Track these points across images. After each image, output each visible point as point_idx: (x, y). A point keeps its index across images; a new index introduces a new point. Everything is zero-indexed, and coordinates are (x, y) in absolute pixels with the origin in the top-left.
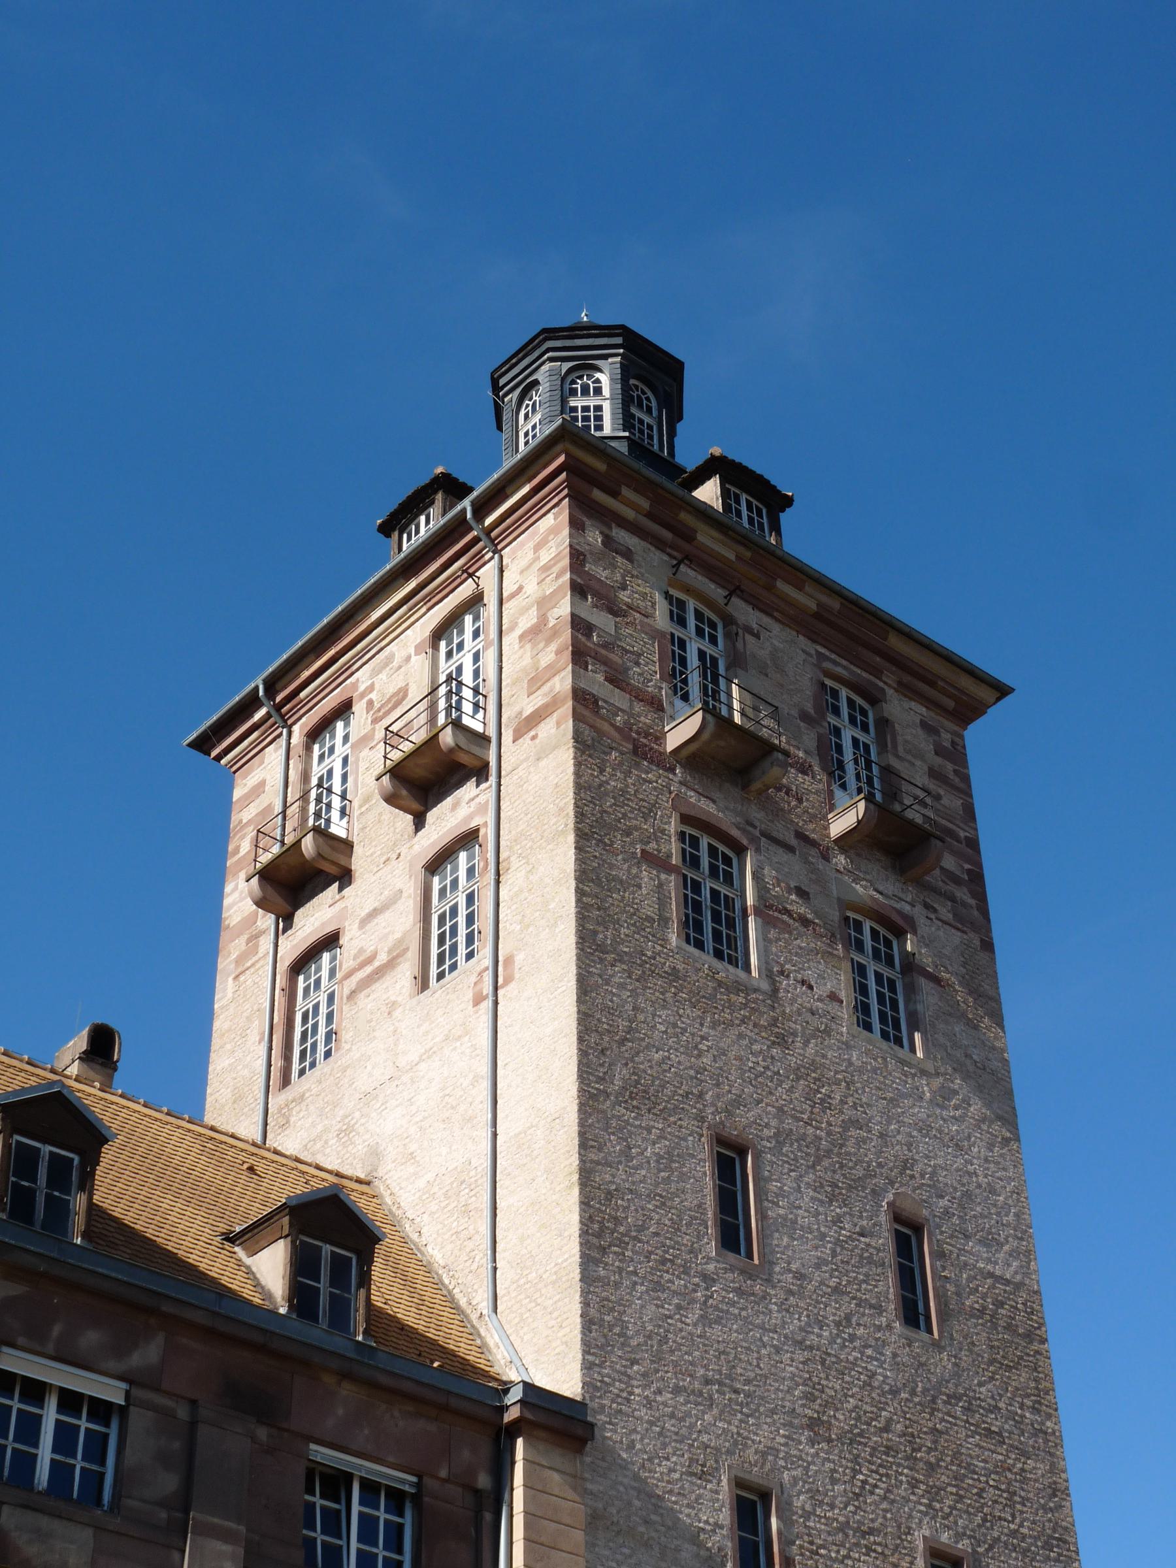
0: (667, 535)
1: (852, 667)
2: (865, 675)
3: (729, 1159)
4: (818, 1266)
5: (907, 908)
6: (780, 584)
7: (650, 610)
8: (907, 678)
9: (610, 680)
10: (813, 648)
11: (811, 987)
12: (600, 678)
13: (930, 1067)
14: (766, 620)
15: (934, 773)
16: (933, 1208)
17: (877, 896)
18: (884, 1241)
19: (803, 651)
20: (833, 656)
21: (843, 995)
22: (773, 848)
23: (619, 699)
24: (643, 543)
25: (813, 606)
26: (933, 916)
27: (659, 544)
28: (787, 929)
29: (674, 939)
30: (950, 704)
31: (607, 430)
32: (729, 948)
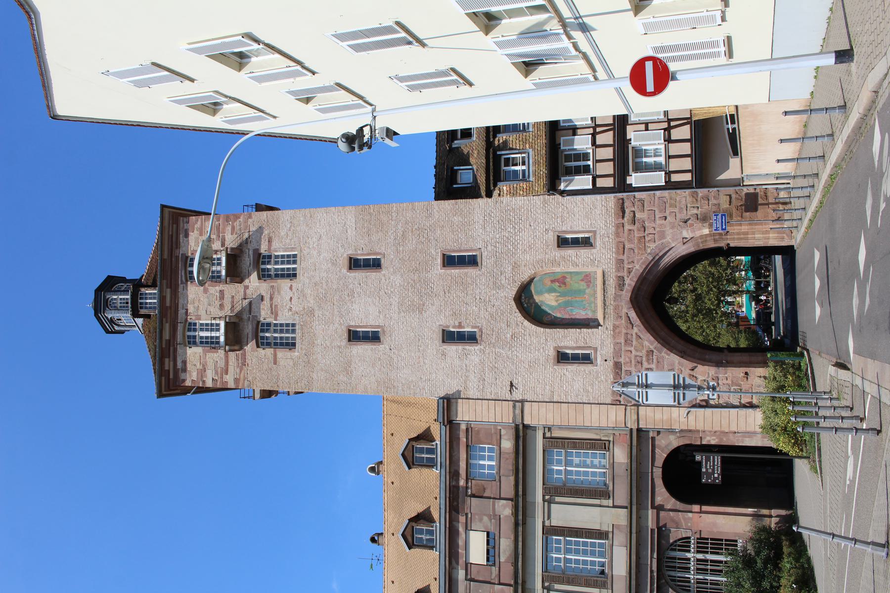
0: (172, 348)
3: (354, 336)
5: (251, 253)
6: (168, 304)
8: (174, 246)
9: (227, 374)
10: (181, 286)
13: (299, 248)
14: (180, 306)
16: (344, 254)
18: (359, 275)
25: (169, 290)
27: (175, 350)
28: (276, 306)
29: (296, 354)
30: (175, 226)
31: (129, 297)
32: (291, 327)
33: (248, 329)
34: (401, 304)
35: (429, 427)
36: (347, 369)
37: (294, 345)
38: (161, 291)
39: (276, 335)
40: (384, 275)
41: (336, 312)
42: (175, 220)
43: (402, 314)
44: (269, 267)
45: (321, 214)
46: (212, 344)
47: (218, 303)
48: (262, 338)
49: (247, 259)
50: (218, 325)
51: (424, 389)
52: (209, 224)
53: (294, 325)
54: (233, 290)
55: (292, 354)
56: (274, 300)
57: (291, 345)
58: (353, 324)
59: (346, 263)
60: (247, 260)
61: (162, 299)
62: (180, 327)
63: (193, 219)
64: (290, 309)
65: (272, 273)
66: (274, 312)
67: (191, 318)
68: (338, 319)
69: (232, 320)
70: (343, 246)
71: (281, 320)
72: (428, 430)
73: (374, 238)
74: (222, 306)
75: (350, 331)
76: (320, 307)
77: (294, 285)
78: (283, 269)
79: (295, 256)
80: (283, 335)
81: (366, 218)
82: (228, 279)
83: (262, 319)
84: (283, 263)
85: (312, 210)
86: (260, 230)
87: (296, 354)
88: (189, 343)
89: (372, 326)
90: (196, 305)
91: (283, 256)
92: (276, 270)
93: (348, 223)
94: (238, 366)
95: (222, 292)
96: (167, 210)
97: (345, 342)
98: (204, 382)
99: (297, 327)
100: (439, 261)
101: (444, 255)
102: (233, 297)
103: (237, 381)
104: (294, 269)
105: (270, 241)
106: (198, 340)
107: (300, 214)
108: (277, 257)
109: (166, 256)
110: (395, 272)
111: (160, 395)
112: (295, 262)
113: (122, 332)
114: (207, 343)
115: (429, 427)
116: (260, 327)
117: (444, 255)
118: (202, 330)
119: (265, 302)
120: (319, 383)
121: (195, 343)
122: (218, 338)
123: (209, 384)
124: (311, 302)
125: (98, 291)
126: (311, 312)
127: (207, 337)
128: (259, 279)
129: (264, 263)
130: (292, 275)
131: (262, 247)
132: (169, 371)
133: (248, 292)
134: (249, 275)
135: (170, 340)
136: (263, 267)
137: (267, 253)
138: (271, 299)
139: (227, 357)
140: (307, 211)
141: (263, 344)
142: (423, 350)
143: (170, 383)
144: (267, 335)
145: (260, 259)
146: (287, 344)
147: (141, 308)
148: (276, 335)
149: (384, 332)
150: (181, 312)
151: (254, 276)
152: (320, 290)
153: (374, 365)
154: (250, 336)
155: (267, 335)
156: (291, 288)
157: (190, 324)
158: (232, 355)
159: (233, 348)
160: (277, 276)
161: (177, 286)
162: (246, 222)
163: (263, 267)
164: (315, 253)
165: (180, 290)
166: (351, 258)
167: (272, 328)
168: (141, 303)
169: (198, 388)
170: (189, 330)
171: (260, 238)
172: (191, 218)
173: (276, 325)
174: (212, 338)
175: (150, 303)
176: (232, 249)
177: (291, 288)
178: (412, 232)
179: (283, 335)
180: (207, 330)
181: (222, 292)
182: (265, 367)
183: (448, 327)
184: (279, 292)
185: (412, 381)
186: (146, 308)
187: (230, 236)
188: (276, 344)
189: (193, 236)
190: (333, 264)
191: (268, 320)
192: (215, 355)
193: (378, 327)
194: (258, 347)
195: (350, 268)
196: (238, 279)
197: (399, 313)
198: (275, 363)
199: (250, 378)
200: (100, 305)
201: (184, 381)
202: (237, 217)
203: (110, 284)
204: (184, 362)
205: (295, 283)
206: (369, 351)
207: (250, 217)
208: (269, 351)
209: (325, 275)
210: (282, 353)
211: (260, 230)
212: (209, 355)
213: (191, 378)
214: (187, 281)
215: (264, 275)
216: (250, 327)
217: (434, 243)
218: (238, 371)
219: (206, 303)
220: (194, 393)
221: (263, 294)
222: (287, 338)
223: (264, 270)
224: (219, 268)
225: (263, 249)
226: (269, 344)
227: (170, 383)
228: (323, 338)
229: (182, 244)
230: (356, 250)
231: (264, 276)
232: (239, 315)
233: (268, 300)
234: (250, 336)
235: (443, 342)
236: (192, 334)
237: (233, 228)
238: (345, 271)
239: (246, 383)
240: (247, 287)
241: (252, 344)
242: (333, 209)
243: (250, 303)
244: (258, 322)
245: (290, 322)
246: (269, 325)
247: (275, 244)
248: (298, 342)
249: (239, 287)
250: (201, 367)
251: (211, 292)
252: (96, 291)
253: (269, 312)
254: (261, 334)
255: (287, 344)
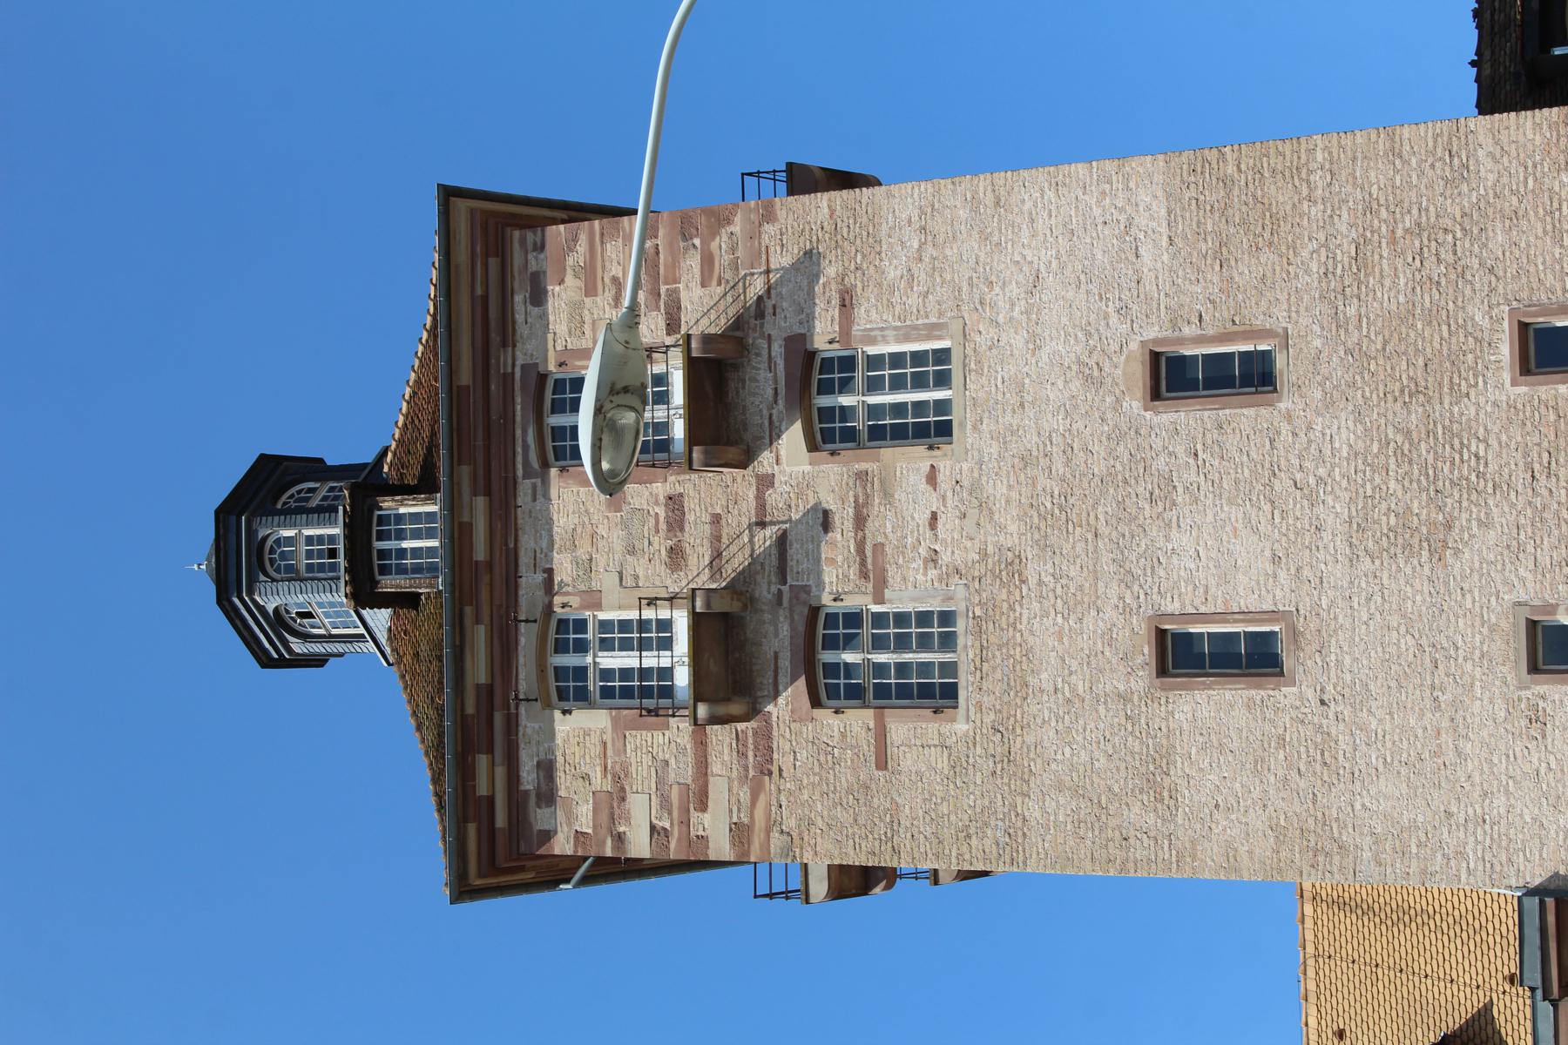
0: (498, 718)
1: (518, 418)
2: (518, 400)
3: (1180, 655)
4: (1255, 530)
5: (778, 349)
6: (480, 554)
7: (595, 739)
8: (495, 338)
9: (703, 806)
10: (525, 486)
11: (934, 517)
12: (707, 818)
13: (956, 327)
14: (524, 559)
15: (590, 290)
17: (781, 402)
18: (1190, 419)
19: (535, 500)
20: (519, 450)
21: (925, 468)
22: (791, 563)
23: (718, 789)
24: (522, 745)
25: (481, 502)
26: (769, 304)
27: (512, 724)
28: (879, 548)
29: (961, 727)
30: (493, 262)
33: (777, 637)
34: (1359, 525)
35: (1488, 1007)
36: (1156, 782)
37: (950, 692)
38: (452, 507)
39: (881, 658)
40: (1289, 417)
41: (1107, 566)
42: (492, 241)
43: (1366, 564)
44: (846, 400)
45: (1032, 190)
46: (644, 696)
47: (661, 544)
48: (832, 669)
49: (764, 375)
50: (665, 625)
51: (1461, 854)
52: (621, 253)
53: (947, 618)
54: (715, 494)
55: (946, 728)
56: (871, 525)
57: (939, 694)
58: (1173, 607)
59: (1139, 374)
60: (765, 379)
61: (457, 534)
62: (526, 638)
63: (558, 233)
64: (933, 559)
65: (860, 423)
66: (873, 573)
67: (567, 604)
68: (1114, 590)
69: (719, 606)
70: (1123, 311)
71: (900, 600)
72: (1484, 1016)
73: (1245, 272)
74: (676, 556)
75: (1161, 634)
76: (1044, 546)
77: (945, 467)
78: (898, 409)
79: (942, 356)
80: (907, 657)
81: (1211, 197)
82: (697, 453)
83: (826, 599)
84: (898, 384)
85: (999, 178)
86: (809, 261)
87: (958, 726)
88: (562, 695)
89: (1247, 615)
90: (582, 553)
91: (897, 359)
92: (874, 411)
93: (1142, 220)
94: (744, 778)
95: (675, 503)
96: (461, 206)
97: (1143, 677)
98: (620, 839)
99: (960, 626)
100: (1505, 351)
101: (1524, 327)
102: (716, 519)
103: (740, 833)
104: (943, 406)
105: (846, 304)
106: (594, 684)
107: (955, 197)
108: (874, 362)
109: (465, 378)
110: (1329, 404)
111: (463, 891)
112: (943, 380)
113: (318, 661)
114: (627, 693)
115: (1488, 1007)
116: (823, 629)
117: (1524, 327)
118: (606, 645)
119: (835, 535)
120: (1053, 835)
121: (582, 697)
122: (666, 673)
123: (640, 846)
124: (1012, 532)
125: (227, 513)
126: (1012, 568)
127: (626, 673)
128: (812, 447)
129: (826, 388)
130: (934, 429)
131: (819, 327)
132: (491, 800)
133: (773, 498)
134: (774, 435)
135: (490, 688)
136: (824, 401)
137: (836, 351)
138: (860, 521)
139: (701, 744)
140: (983, 182)
141: (833, 692)
142: (1455, 704)
143: (497, 847)
144: (849, 657)
145: (813, 375)
146: (926, 692)
147: (384, 570)
148: (881, 658)
149: (1295, 634)
150: (530, 581)
151: (793, 437)
152: (1043, 481)
153: (1259, 766)
154: (785, 663)
155: (849, 657)
156: (932, 478)
157: (563, 624)
158: (721, 736)
159: (722, 710)
160: (877, 434)
161: (510, 486)
162: (754, 235)
163: (824, 401)
164: (1018, 341)
165: (523, 498)
166: (1155, 357)
167: (867, 631)
168: (383, 554)
169: (600, 861)
170: (561, 647)
171: (811, 295)
172: (551, 230)
173: (879, 620)
174: (644, 673)
175: (416, 552)
176: (707, 339)
177: (932, 478)
178: (1393, 241)
179: (907, 657)
180: (626, 645)
181: (675, 503)
182: (845, 777)
183: (1552, 609)
184: (887, 494)
185: (1413, 826)
186: (402, 570)
187: (698, 291)
188: (882, 692)
189: (562, 297)
190: (1088, 379)
191: (851, 603)
192: (659, 737)
193: (1273, 615)
194: (816, 703)
195: (1156, 395)
196: (732, 453)
197: (1353, 560)
198: (882, 764)
199: (790, 823)
200: (237, 563)
201: (547, 836)
202: (720, 219)
203: (271, 484)
204: (547, 768)
205: (946, 460)
206: (1240, 716)
207: (768, 216)
208: (859, 720)
209: (1059, 423)
210: (905, 726)
211: (809, 261)
212: (636, 738)
213: (572, 825)
214: (545, 465)
215: (830, 434)
216: (785, 630)
217: (1480, 280)
218: (744, 795)
219: (619, 547)
220: (587, 880)
221: (830, 503)
222: (925, 668)
223: (827, 414)
224: (660, 414)
225: (824, 335)
226: (856, 694)
227: (497, 847)
228: (1063, 659)
229: (522, 330)
230: (1174, 325)
231: (828, 437)
232: (741, 587)
233: (849, 525)
234: (785, 663)
235: (1534, 669)
236: (570, 660)
237: (708, 261)
238: (1134, 404)
239: (776, 840)
240: (766, 482)
241: (793, 695)
242: (1080, 169)
243: (782, 541)
244: (815, 611)
245: (934, 605)
246: (854, 619)
247: (867, 316)
248: (965, 680)
249: (741, 482)
250: (608, 786)
251: (637, 502)
252: (218, 512)
253: (853, 573)
254: (827, 657)
255: (926, 692)
